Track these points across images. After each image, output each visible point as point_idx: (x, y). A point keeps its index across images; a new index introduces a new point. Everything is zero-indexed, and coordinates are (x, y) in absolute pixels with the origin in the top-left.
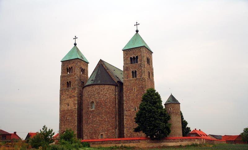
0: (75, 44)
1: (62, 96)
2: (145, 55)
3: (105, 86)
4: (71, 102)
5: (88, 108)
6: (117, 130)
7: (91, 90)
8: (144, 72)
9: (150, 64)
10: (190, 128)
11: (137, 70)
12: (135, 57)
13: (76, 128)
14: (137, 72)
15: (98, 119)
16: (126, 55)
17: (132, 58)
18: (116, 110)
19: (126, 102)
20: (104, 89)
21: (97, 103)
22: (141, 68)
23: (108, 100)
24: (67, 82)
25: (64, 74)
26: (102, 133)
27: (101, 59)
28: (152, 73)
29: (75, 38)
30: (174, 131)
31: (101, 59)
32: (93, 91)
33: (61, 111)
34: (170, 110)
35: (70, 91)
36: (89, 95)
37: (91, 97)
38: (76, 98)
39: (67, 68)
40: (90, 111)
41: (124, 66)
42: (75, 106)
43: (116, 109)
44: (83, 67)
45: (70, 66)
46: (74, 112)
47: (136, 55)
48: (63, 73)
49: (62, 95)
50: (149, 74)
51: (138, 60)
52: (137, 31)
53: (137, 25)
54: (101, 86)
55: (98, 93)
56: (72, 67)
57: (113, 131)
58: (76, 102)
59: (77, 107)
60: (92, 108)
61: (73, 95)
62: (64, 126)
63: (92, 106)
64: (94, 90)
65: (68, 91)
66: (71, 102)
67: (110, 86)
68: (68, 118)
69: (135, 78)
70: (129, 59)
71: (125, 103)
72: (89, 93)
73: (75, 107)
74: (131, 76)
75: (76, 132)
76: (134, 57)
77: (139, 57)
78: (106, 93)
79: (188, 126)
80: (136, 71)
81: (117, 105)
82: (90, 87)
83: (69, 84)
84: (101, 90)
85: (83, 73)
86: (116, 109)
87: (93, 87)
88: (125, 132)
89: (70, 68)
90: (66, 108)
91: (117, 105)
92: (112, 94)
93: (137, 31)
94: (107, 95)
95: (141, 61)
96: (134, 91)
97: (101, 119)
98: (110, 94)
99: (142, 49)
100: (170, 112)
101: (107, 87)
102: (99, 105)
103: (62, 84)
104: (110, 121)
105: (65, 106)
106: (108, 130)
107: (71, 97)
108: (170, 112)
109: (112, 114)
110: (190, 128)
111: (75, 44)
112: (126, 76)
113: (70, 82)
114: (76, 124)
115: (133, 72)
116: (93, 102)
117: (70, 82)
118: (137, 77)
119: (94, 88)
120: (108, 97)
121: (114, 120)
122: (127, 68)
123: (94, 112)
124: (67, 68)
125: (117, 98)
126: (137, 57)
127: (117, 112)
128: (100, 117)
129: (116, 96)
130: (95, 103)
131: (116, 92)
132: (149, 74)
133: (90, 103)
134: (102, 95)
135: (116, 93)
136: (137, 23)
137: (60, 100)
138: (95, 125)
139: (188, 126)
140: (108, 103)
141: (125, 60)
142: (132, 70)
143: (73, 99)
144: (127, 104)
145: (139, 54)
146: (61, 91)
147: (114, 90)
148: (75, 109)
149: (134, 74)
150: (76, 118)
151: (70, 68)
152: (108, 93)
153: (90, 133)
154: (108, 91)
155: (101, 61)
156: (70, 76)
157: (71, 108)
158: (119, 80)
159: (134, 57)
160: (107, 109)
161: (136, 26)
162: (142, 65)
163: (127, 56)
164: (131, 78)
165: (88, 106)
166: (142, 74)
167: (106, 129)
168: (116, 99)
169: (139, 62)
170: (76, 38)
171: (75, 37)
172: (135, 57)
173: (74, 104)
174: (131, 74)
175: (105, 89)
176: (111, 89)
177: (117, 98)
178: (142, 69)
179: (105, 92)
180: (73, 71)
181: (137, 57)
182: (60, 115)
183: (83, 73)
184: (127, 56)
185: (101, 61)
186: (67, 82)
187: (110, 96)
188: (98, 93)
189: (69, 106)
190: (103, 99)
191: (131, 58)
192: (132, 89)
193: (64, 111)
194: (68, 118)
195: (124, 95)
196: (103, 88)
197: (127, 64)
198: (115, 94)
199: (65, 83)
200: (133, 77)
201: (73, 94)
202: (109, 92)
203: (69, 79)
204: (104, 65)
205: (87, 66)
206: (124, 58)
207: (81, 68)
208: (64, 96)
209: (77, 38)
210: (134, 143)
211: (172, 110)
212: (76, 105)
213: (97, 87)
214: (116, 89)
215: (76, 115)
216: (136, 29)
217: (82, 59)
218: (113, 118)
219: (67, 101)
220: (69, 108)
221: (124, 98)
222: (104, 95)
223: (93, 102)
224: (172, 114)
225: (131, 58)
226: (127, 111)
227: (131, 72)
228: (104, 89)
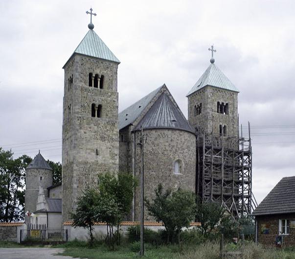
0: (91, 27)
17: (221, 103)
24: (93, 105)
27: (165, 84)
31: (165, 84)
32: (181, 142)
36: (173, 146)
38: (117, 144)
42: (113, 158)
47: (227, 102)
48: (81, 81)
49: (81, 128)
58: (117, 152)
59: (118, 160)
64: (183, 140)
65: (97, 125)
66: (104, 148)
72: (174, 144)
73: (113, 161)
76: (223, 103)
77: (230, 106)
82: (175, 132)
87: (181, 135)
105: (89, 153)
107: (103, 139)
111: (91, 27)
113: (100, 107)
119: (183, 136)
143: (109, 145)
148: (114, 164)
151: (97, 75)
157: (104, 160)
159: (223, 103)
163: (213, 98)
165: (171, 167)
169: (231, 115)
171: (87, 12)
172: (225, 104)
181: (227, 104)
185: (164, 86)
191: (218, 103)
193: (86, 163)
208: (85, 133)
212: (117, 158)
223: (179, 161)
225: (218, 103)
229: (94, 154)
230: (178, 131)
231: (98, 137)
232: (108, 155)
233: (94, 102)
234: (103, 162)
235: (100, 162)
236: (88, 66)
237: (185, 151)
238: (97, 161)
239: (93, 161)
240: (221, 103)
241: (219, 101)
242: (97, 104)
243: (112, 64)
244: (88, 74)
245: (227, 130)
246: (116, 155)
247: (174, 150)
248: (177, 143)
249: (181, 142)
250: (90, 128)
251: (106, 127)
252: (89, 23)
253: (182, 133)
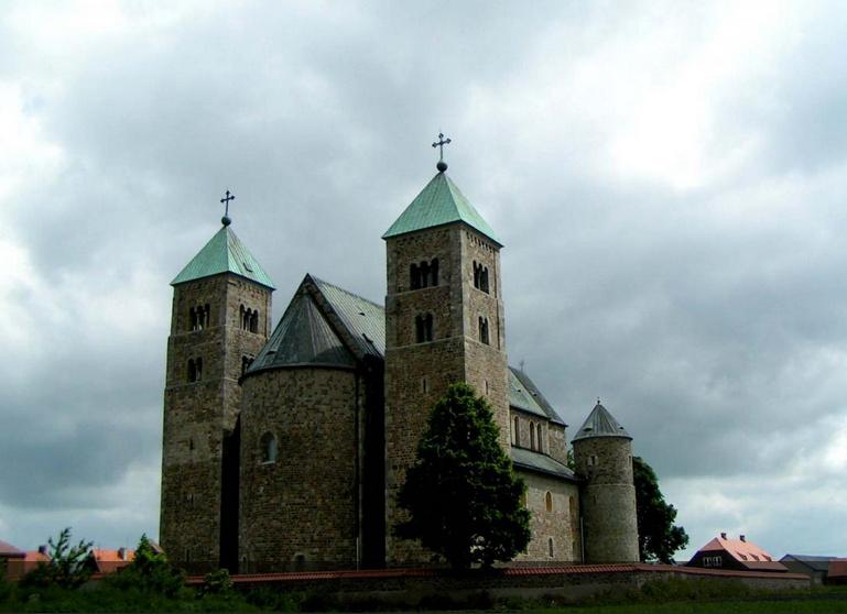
1: (173, 412)
2: (469, 254)
3: (316, 373)
4: (200, 434)
5: (253, 457)
6: (358, 541)
7: (265, 392)
8: (461, 318)
9: (491, 289)
10: (682, 529)
11: (433, 313)
12: (429, 264)
13: (217, 533)
14: (435, 324)
15: (285, 497)
16: (395, 255)
17: (418, 266)
18: (358, 466)
19: (391, 435)
20: (309, 386)
21: (284, 439)
22: (449, 305)
23: (326, 425)
24: (191, 361)
25: (181, 334)
26: (300, 554)
27: (308, 275)
28: (498, 323)
29: (228, 199)
30: (606, 543)
31: (308, 275)
32: (272, 393)
33: (166, 471)
34: (590, 463)
35: (197, 396)
37: (263, 415)
39: (192, 309)
40: (259, 470)
41: (387, 298)
42: (213, 450)
43: (357, 460)
44: (252, 304)
45: (201, 301)
46: (211, 473)
49: (172, 408)
50: (484, 327)
51: (440, 274)
52: (442, 167)
53: (441, 143)
54: (300, 374)
55: (290, 401)
56: (208, 306)
57: (346, 543)
58: (219, 436)
59: (221, 452)
60: (267, 459)
61: (208, 409)
62: (175, 524)
63: (266, 450)
64: (276, 389)
66: (200, 434)
67: (334, 374)
68: (189, 497)
69: (427, 343)
70: (407, 270)
71: (388, 436)
74: (413, 335)
75: (218, 547)
76: (424, 263)
78: (318, 402)
79: (677, 523)
80: (429, 317)
81: (361, 446)
83: (194, 368)
84: (298, 388)
85: (253, 329)
86: (357, 460)
87: (271, 380)
88: (387, 547)
89: (200, 308)
90: (183, 456)
91: (361, 446)
92: (341, 403)
93: (442, 167)
94: (323, 408)
95: (449, 280)
96: (422, 391)
97: (297, 500)
98: (334, 403)
99: (451, 234)
100: (590, 473)
101: (322, 376)
102: (291, 444)
103: (173, 368)
104: (333, 507)
105: (181, 450)
106: (324, 543)
107: (200, 418)
108: (590, 473)
109: (343, 481)
110: (682, 529)
112: (395, 337)
113: (199, 359)
114: (217, 518)
115: (418, 319)
116: (267, 438)
117: (199, 359)
118: (435, 340)
120: (327, 415)
121: (348, 501)
122: (399, 305)
123: (274, 473)
124: (192, 309)
125: (363, 421)
126: (435, 262)
127: (360, 473)
128: (293, 489)
129: (357, 413)
130: (276, 437)
131: (357, 395)
132: (484, 327)
133: (259, 438)
134: (303, 409)
135: (360, 402)
136: (441, 136)
137: (165, 429)
138: (274, 523)
139: (677, 523)
140: (326, 437)
141: (393, 272)
142: (415, 313)
143: (206, 425)
144: (396, 443)
145: (443, 252)
146: (169, 392)
147: (349, 388)
148: (215, 460)
149: (424, 326)
150: (218, 498)
151: (200, 308)
152: (326, 401)
153: (257, 550)
154: (325, 392)
155: (308, 280)
156: (200, 337)
157: (201, 457)
158: (373, 352)
159: (424, 263)
160: (322, 462)
161: (438, 141)
162: (451, 293)
163: (400, 261)
164: (414, 344)
166: (452, 327)
167: (316, 537)
168: (357, 426)
169: (442, 283)
170: (228, 198)
171: (228, 193)
172: (429, 264)
173: (213, 443)
174: (414, 327)
175: (316, 387)
176: (339, 385)
177: (360, 418)
178: (452, 308)
179: (314, 398)
180: (212, 320)
181: (435, 262)
182: (163, 483)
183: (253, 329)
184: (400, 261)
186: (191, 361)
187: (332, 413)
188: (290, 401)
189: (195, 452)
190: (306, 423)
191: (413, 266)
192: (416, 386)
193: (177, 468)
194: (189, 497)
195: (387, 408)
196: (310, 381)
197: (400, 291)
198: (353, 402)
199: (183, 366)
200: (420, 339)
201: (209, 405)
202: (328, 397)
203: (197, 350)
204: (318, 295)
205: (267, 302)
206: (388, 266)
207: (242, 307)
209: (233, 198)
210: (384, 590)
211: (597, 463)
212: (219, 447)
213: (284, 377)
214: (357, 384)
215: (218, 483)
216: (438, 161)
217: (246, 274)
218: (346, 496)
219: (185, 434)
220: (195, 456)
221: (388, 420)
222: (310, 406)
223: (267, 438)
224: (600, 478)
226: (395, 467)
227: (413, 320)
228: (309, 386)
229: (187, 448)
230: (266, 374)
231: (193, 416)
232: (207, 446)
233: (190, 357)
234: (199, 460)
235: (195, 461)
236: (188, 298)
237: (279, 411)
238: (191, 460)
239: (185, 461)
240: (418, 266)
241: (415, 261)
242: (195, 357)
243: (219, 279)
244: (188, 310)
245: (434, 321)
246: (219, 442)
247: (259, 415)
248: (264, 398)
249: (272, 393)
250: (183, 403)
251: (205, 395)
252: (224, 215)
253: (273, 376)
